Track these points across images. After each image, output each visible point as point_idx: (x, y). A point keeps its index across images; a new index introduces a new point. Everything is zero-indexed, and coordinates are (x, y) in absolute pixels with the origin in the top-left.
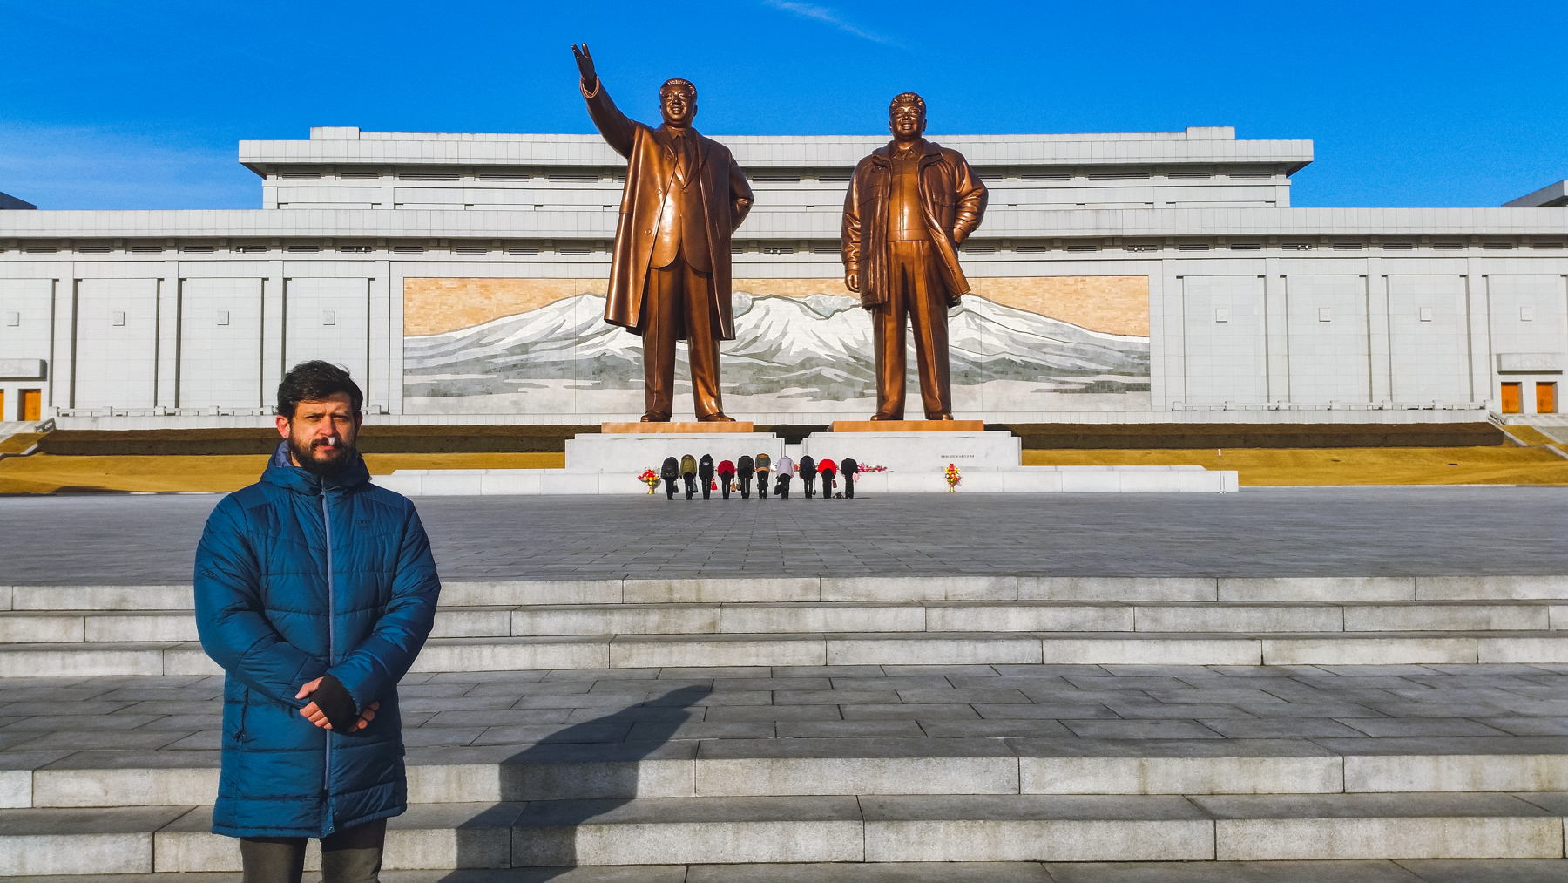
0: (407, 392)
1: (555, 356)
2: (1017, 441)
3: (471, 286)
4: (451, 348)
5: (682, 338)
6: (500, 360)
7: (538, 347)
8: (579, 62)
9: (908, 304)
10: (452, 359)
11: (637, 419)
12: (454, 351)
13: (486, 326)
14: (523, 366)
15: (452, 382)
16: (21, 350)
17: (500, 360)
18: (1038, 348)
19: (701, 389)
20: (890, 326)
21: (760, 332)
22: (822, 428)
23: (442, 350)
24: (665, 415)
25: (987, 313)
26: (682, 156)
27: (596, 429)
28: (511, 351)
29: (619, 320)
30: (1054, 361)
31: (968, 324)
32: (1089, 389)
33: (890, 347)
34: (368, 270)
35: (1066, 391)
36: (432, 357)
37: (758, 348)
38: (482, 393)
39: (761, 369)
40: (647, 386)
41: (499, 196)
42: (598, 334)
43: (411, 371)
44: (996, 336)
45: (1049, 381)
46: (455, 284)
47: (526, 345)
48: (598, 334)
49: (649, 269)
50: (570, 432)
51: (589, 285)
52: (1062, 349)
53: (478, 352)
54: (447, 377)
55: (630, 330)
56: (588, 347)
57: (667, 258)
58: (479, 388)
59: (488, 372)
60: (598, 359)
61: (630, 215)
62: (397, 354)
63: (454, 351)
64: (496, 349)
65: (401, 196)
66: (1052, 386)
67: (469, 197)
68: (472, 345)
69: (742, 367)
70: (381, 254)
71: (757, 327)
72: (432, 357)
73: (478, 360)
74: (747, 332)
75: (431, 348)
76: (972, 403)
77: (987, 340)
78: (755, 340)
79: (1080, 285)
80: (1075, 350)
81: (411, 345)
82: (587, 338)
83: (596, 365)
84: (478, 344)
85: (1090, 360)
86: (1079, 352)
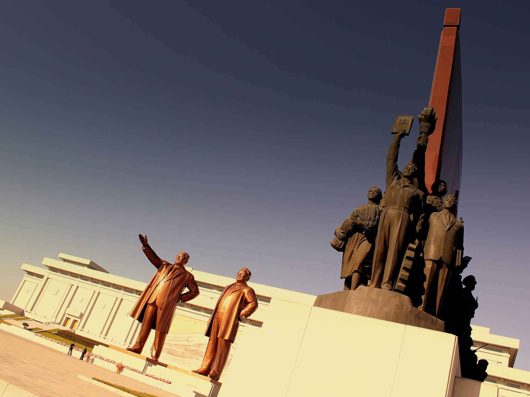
4: (179, 339)
6: (191, 347)
16: (76, 309)
22: (165, 366)
27: (107, 346)
29: (133, 315)
38: (182, 357)
50: (98, 343)
53: (186, 343)
54: (174, 348)
57: (152, 301)
58: (181, 354)
59: (186, 350)
64: (190, 343)
73: (184, 345)
75: (174, 337)
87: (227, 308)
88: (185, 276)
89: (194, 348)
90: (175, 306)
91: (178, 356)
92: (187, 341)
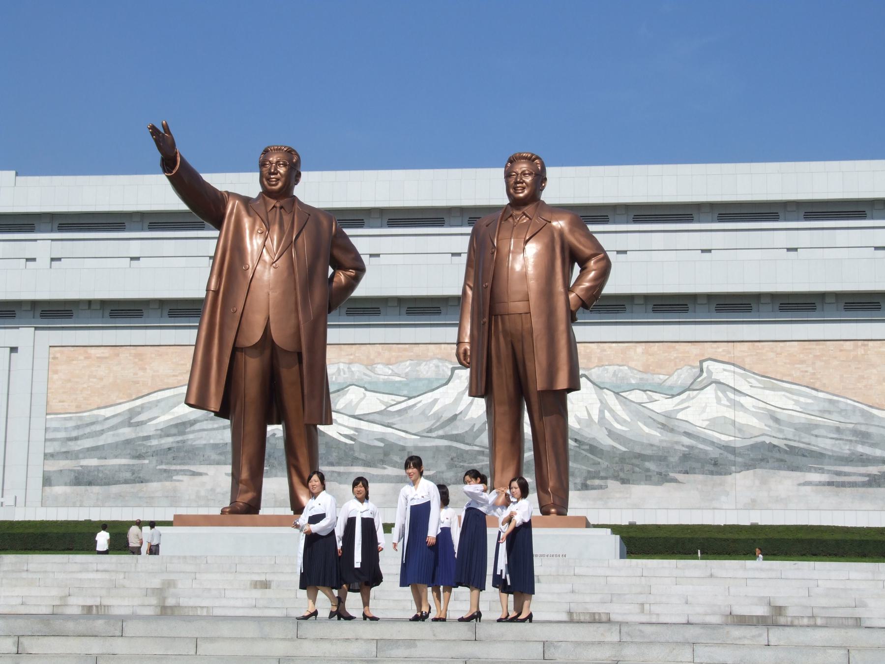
0: (47, 481)
2: (618, 537)
3: (125, 353)
4: (98, 428)
5: (279, 423)
6: (154, 442)
7: (197, 427)
8: (157, 141)
9: (521, 388)
10: (101, 441)
11: (217, 511)
12: (102, 432)
13: (139, 402)
14: (179, 449)
15: (97, 468)
17: (154, 442)
18: (808, 428)
19: (296, 479)
20: (502, 410)
21: (460, 408)
23: (88, 430)
24: (253, 507)
25: (745, 388)
26: (276, 228)
28: (165, 432)
29: (200, 404)
30: (824, 444)
31: (719, 401)
32: (874, 481)
33: (504, 434)
35: (843, 485)
36: (76, 439)
37: (458, 429)
39: (461, 454)
40: (233, 474)
41: (169, 247)
44: (754, 414)
45: (822, 471)
46: (106, 352)
49: (235, 349)
52: (838, 430)
53: (127, 433)
54: (93, 462)
58: (128, 475)
59: (140, 457)
61: (216, 292)
62: (38, 436)
63: (102, 432)
64: (149, 430)
65: (59, 249)
66: (825, 478)
67: (135, 248)
68: (122, 425)
69: (437, 449)
71: (457, 400)
72: (76, 439)
73: (128, 442)
74: (445, 408)
75: (78, 427)
76: (723, 498)
77: (742, 418)
78: (455, 416)
79: (860, 351)
80: (855, 432)
81: (54, 424)
84: (130, 419)
85: (874, 445)
86: (864, 437)
87: (533, 296)
88: (318, 224)
89: (168, 441)
90: (325, 327)
91: (117, 482)
92: (130, 425)
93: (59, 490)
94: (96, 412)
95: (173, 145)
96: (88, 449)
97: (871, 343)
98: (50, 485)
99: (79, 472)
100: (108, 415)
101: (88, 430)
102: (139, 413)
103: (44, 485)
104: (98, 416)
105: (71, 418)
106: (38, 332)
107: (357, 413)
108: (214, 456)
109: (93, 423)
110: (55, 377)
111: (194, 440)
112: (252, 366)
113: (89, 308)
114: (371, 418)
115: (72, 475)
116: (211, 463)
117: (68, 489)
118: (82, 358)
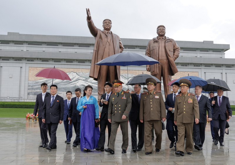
0: (28, 94)
1: (64, 86)
7: (60, 84)
34: (20, 65)
36: (34, 86)
42: (74, 81)
43: (30, 89)
47: (57, 83)
48: (74, 81)
51: (72, 70)
55: (95, 79)
56: (72, 84)
60: (74, 87)
61: (96, 51)
62: (27, 85)
70: (24, 62)
72: (34, 86)
75: (35, 83)
79: (184, 74)
81: (30, 83)
82: (72, 82)
83: (73, 88)
93: (31, 96)
94: (39, 81)
95: (90, 15)
96: (37, 88)
97: (186, 72)
98: (29, 95)
99: (35, 92)
100: (41, 81)
101: (37, 84)
102: (48, 81)
103: (28, 95)
104: (39, 81)
105: (33, 82)
106: (26, 64)
107: (92, 82)
108: (63, 90)
109: (38, 83)
110: (30, 73)
111: (59, 87)
112: (104, 68)
113: (37, 60)
114: (95, 83)
115: (34, 93)
116: (63, 91)
117: (33, 96)
118: (36, 70)
